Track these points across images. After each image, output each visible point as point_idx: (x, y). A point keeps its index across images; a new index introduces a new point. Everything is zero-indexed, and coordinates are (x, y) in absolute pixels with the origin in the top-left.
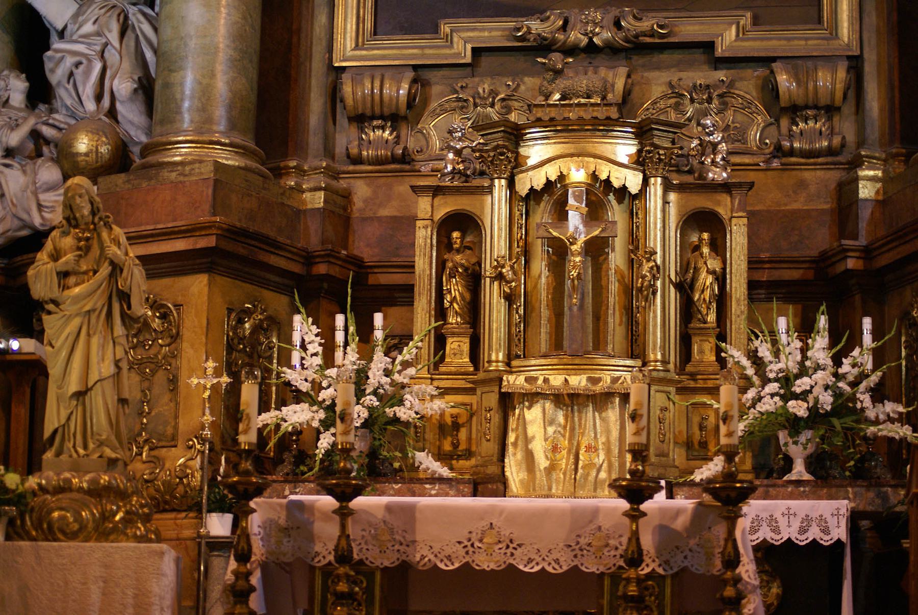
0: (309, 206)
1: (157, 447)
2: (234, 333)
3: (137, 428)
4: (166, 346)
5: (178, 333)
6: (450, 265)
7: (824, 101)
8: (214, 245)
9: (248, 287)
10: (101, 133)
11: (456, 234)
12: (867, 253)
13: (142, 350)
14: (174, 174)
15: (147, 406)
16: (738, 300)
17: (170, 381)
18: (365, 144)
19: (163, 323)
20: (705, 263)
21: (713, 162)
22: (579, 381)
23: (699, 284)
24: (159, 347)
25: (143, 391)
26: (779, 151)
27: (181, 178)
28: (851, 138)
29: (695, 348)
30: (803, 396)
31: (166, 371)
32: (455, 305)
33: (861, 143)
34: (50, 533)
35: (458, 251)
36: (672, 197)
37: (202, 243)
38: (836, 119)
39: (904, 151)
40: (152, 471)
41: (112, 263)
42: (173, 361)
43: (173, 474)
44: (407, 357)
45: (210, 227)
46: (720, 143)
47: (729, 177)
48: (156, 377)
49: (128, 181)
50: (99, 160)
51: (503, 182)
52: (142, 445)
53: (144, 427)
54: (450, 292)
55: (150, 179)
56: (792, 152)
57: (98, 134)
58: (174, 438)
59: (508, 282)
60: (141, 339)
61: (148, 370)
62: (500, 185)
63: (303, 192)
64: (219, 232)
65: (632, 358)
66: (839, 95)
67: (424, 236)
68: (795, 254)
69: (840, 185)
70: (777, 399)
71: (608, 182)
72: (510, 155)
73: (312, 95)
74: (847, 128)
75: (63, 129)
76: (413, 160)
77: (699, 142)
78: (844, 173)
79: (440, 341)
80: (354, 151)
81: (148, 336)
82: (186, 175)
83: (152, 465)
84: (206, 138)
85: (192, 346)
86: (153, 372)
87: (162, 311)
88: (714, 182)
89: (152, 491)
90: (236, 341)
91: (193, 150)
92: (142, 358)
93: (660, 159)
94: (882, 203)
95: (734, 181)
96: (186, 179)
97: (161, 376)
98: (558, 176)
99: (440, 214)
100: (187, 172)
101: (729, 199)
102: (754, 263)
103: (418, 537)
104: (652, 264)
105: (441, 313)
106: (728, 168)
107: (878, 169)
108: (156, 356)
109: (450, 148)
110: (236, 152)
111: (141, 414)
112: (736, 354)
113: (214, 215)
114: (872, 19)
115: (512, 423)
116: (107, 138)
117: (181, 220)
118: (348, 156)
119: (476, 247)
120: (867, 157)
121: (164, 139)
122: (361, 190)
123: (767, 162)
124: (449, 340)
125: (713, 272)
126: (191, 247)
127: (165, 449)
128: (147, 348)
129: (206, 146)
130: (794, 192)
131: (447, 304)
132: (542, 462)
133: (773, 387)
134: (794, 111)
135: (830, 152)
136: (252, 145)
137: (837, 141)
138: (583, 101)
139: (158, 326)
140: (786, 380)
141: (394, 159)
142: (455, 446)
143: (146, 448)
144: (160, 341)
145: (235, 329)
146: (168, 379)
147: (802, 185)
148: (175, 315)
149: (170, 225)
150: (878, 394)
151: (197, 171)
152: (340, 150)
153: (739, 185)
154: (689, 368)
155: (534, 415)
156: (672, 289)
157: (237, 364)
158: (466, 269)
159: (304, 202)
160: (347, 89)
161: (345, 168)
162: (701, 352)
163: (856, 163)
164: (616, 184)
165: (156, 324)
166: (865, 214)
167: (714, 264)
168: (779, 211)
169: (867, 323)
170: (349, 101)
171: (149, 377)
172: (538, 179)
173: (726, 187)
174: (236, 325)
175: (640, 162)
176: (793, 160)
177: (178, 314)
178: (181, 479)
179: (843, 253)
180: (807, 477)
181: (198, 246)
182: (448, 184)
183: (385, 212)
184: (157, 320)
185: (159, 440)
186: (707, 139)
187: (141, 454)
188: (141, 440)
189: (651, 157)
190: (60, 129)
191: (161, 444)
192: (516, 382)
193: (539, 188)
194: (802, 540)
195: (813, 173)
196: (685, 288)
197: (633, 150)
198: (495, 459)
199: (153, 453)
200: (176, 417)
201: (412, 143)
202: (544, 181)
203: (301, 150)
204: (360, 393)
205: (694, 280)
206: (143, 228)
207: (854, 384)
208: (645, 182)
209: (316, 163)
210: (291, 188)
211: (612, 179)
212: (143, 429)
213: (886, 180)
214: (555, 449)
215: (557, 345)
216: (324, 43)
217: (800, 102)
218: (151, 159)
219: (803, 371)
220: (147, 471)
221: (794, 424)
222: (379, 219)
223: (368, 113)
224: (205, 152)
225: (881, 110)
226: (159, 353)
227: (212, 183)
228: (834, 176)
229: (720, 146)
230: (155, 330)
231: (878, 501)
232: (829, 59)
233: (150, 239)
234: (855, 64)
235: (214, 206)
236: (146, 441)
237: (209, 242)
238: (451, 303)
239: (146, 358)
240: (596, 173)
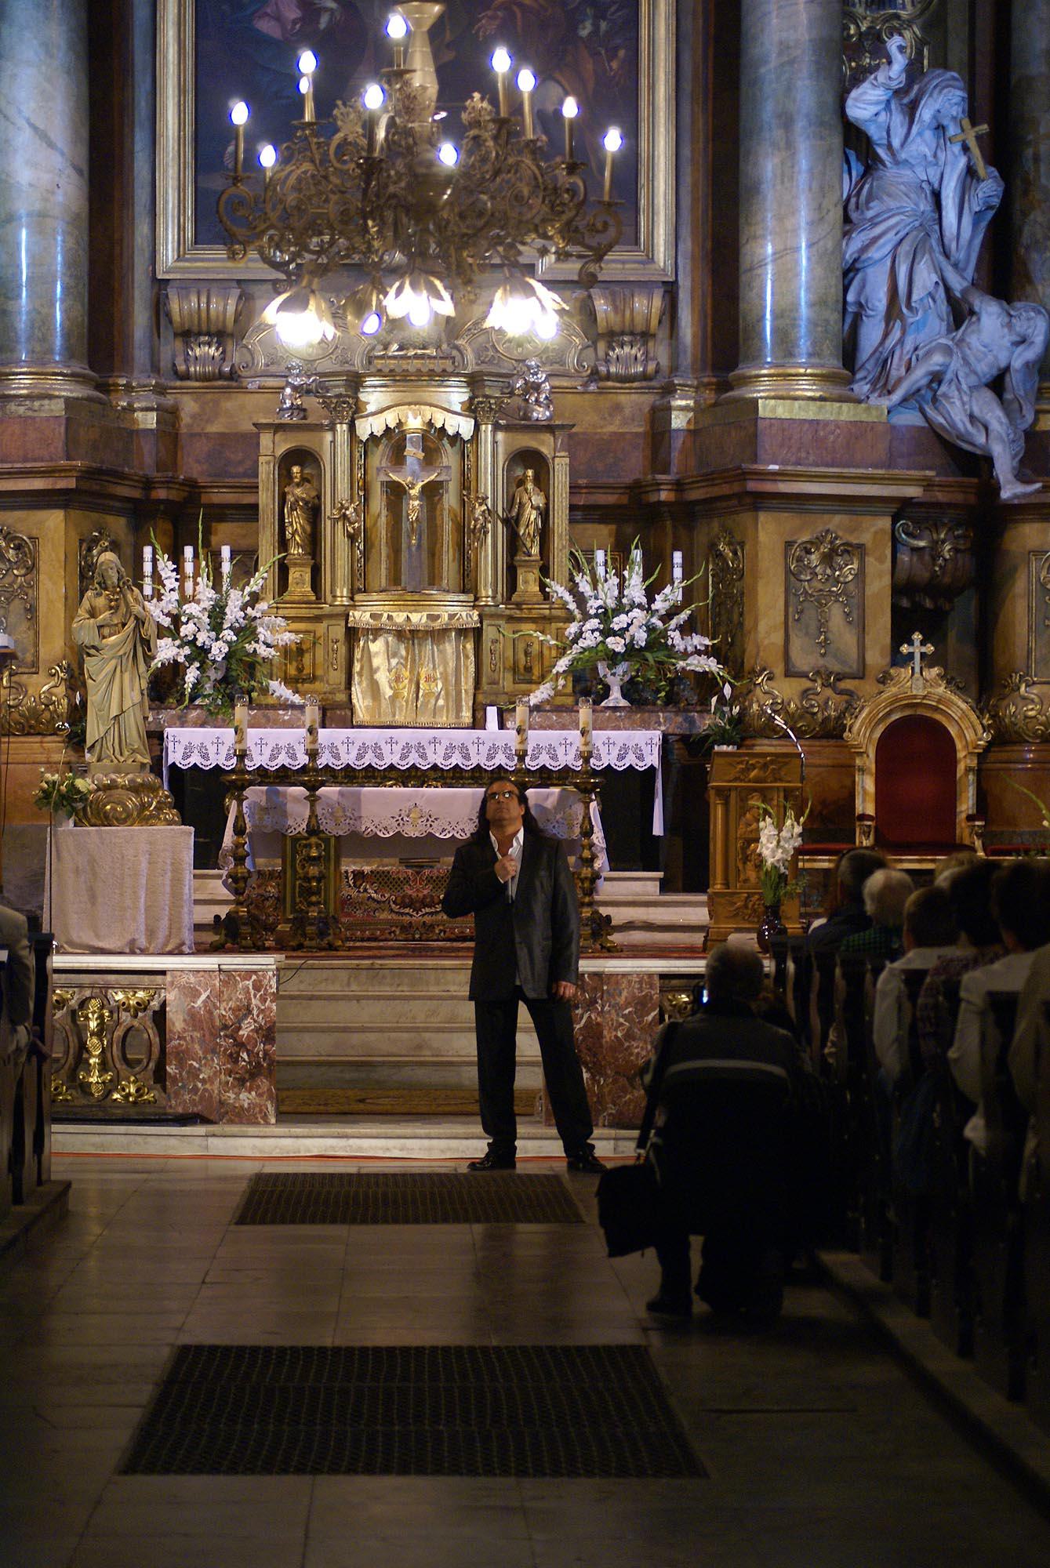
0: (142, 426)
5: (34, 564)
6: (290, 498)
7: (640, 326)
8: (74, 486)
9: (94, 516)
11: (296, 469)
12: (679, 486)
16: (560, 536)
18: (192, 359)
20: (530, 499)
21: (537, 400)
22: (418, 618)
26: (595, 376)
28: (664, 360)
29: (520, 579)
30: (621, 633)
32: (297, 538)
33: (674, 369)
34: (106, 820)
35: (298, 485)
36: (500, 436)
37: (61, 484)
38: (651, 344)
39: (714, 380)
41: (136, 618)
42: (30, 591)
44: (255, 588)
45: (70, 470)
46: (543, 382)
48: (11, 607)
51: (345, 427)
54: (292, 525)
56: (608, 377)
59: (351, 523)
62: (342, 429)
63: (135, 410)
65: (463, 592)
66: (654, 322)
67: (267, 471)
68: (611, 480)
69: (654, 410)
70: (597, 634)
71: (443, 429)
72: (351, 401)
73: (136, 307)
74: (661, 354)
76: (239, 376)
78: (657, 397)
79: (283, 570)
85: (50, 579)
93: (491, 409)
94: (693, 433)
99: (280, 451)
102: (574, 489)
103: (363, 814)
104: (484, 508)
105: (283, 544)
107: (690, 399)
108: (11, 585)
109: (288, 384)
112: (559, 590)
114: (687, 245)
115: (358, 655)
118: (176, 372)
119: (313, 479)
120: (680, 385)
122: (189, 406)
123: (585, 385)
124: (292, 571)
125: (537, 508)
126: (50, 487)
130: (610, 415)
131: (288, 536)
132: (388, 692)
133: (594, 623)
134: (612, 337)
135: (644, 377)
136: (81, 367)
137: (651, 367)
138: (419, 352)
140: (606, 615)
141: (221, 376)
142: (300, 670)
144: (15, 572)
145: (85, 557)
147: (617, 408)
150: (686, 629)
152: (165, 364)
153: (562, 427)
154: (514, 598)
155: (377, 647)
156: (500, 525)
158: (306, 503)
159: (135, 421)
160: (175, 306)
161: (172, 384)
162: (526, 582)
163: (669, 390)
164: (451, 431)
166: (678, 443)
167: (538, 500)
168: (596, 434)
169: (678, 557)
170: (176, 318)
173: (549, 428)
175: (471, 409)
176: (610, 384)
178: (47, 706)
179: (657, 486)
180: (623, 703)
181: (58, 487)
183: (214, 428)
191: (20, 670)
192: (361, 617)
193: (379, 435)
194: (620, 766)
195: (628, 396)
196: (512, 524)
197: (465, 397)
198: (343, 687)
200: (36, 645)
201: (237, 357)
203: (127, 365)
204: (216, 627)
207: (667, 617)
209: (146, 381)
210: (124, 408)
213: (698, 410)
214: (398, 679)
215: (395, 579)
216: (147, 254)
217: (617, 328)
219: (620, 609)
221: (613, 658)
222: (207, 435)
223: (195, 329)
225: (694, 336)
226: (14, 582)
227: (64, 422)
228: (647, 400)
230: (9, 560)
231: (686, 725)
232: (646, 286)
234: (671, 290)
237: (71, 483)
238: (293, 535)
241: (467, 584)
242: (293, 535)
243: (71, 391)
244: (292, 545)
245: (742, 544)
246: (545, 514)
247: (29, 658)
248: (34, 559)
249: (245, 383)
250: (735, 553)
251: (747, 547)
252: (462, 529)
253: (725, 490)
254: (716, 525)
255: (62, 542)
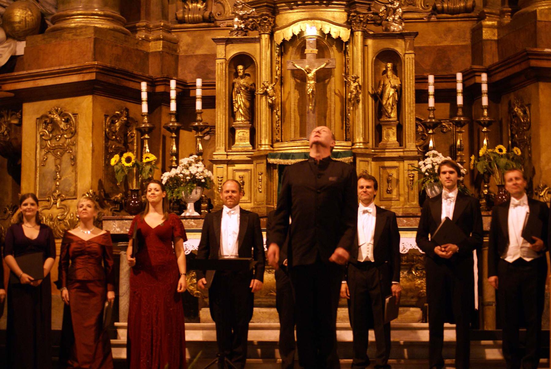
1: (65, 199)
2: (109, 130)
3: (54, 187)
4: (69, 138)
5: (76, 131)
6: (237, 86)
9: (117, 102)
10: (28, 9)
11: (240, 67)
13: (55, 140)
14: (71, 35)
15: (59, 174)
16: (410, 104)
17: (72, 159)
18: (187, 11)
19: (67, 125)
20: (390, 82)
21: (394, 20)
23: (386, 96)
24: (65, 139)
25: (56, 166)
27: (75, 37)
29: (384, 133)
31: (69, 154)
32: (240, 110)
35: (242, 77)
36: (370, 42)
39: (510, 9)
40: (62, 213)
42: (73, 148)
43: (75, 215)
46: (398, 8)
47: (403, 29)
49: (44, 39)
50: (27, 25)
51: (266, 36)
52: (56, 198)
53: (57, 187)
54: (237, 102)
55: (57, 38)
56: (443, 11)
57: (26, 10)
58: (75, 193)
60: (54, 134)
61: (59, 153)
64: (97, 70)
65: (346, 141)
68: (445, 73)
71: (329, 35)
72: (270, 19)
75: (6, 7)
76: (216, 20)
77: (385, 8)
78: (475, 23)
80: (180, 15)
81: (58, 133)
82: (77, 36)
83: (63, 210)
84: (89, 12)
86: (62, 154)
87: (66, 117)
88: (394, 33)
89: (63, 226)
90: (110, 134)
91: (81, 19)
92: (55, 146)
93: (361, 21)
95: (406, 31)
96: (78, 38)
97: (66, 157)
98: (300, 32)
100: (78, 34)
101: (403, 42)
104: (356, 84)
105: (232, 115)
106: (403, 23)
107: (495, 21)
108: (63, 144)
109: (237, 15)
110: (108, 20)
111: (55, 179)
113: (95, 60)
116: (31, 12)
117: (75, 63)
118: (177, 18)
120: (488, 13)
121: (64, 13)
123: (429, 18)
124: (238, 131)
125: (394, 87)
126: (81, 80)
127: (70, 201)
128: (58, 140)
129: (89, 17)
130: (445, 35)
131: (235, 110)
135: (466, 10)
136: (118, 15)
139: (64, 127)
141: (204, 20)
143: (59, 200)
144: (65, 136)
145: (110, 127)
146: (71, 158)
148: (74, 120)
149: (68, 67)
151: (84, 33)
153: (409, 34)
156: (370, 98)
157: (111, 148)
158: (247, 88)
162: (388, 135)
163: (482, 17)
164: (334, 36)
165: (62, 125)
167: (395, 82)
168: (436, 47)
171: (59, 157)
172: (288, 33)
173: (401, 36)
174: (110, 124)
176: (444, 15)
177: (75, 119)
181: (86, 79)
182: (235, 37)
183: (199, 52)
184: (63, 123)
185: (67, 195)
186: (390, 6)
187: (56, 204)
188: (56, 195)
189: (355, 19)
190: (4, 7)
191: (67, 198)
195: (456, 23)
199: (63, 203)
201: (214, 9)
202: (291, 35)
205: (383, 92)
206: (53, 68)
208: (352, 33)
209: (158, 23)
210: (143, 39)
211: (331, 33)
212: (57, 188)
218: (58, 25)
220: (60, 214)
222: (196, 56)
224: (89, 21)
226: (65, 142)
227: (93, 40)
229: (398, 10)
230: (62, 129)
233: (57, 75)
235: (94, 54)
236: (59, 195)
237: (91, 76)
239: (58, 146)
240: (322, 30)
241: (348, 136)
242: (238, 109)
243: (102, 24)
244: (238, 114)
245: (529, 105)
246: (399, 91)
247: (72, 189)
248: (75, 127)
249: (218, 23)
250: (525, 112)
251: (532, 106)
252: (344, 101)
253: (517, 69)
254: (512, 97)
255: (91, 115)
